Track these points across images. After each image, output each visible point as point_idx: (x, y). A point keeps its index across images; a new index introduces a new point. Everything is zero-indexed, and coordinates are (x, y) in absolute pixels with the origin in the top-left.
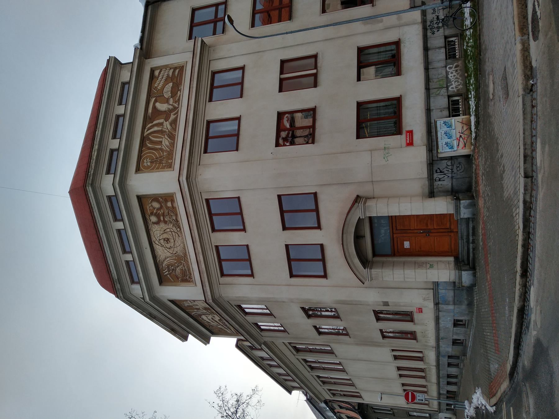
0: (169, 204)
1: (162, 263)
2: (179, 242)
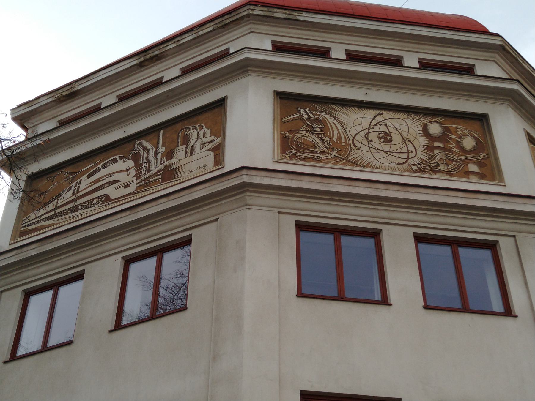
0: (473, 168)
1: (329, 114)
2: (383, 159)
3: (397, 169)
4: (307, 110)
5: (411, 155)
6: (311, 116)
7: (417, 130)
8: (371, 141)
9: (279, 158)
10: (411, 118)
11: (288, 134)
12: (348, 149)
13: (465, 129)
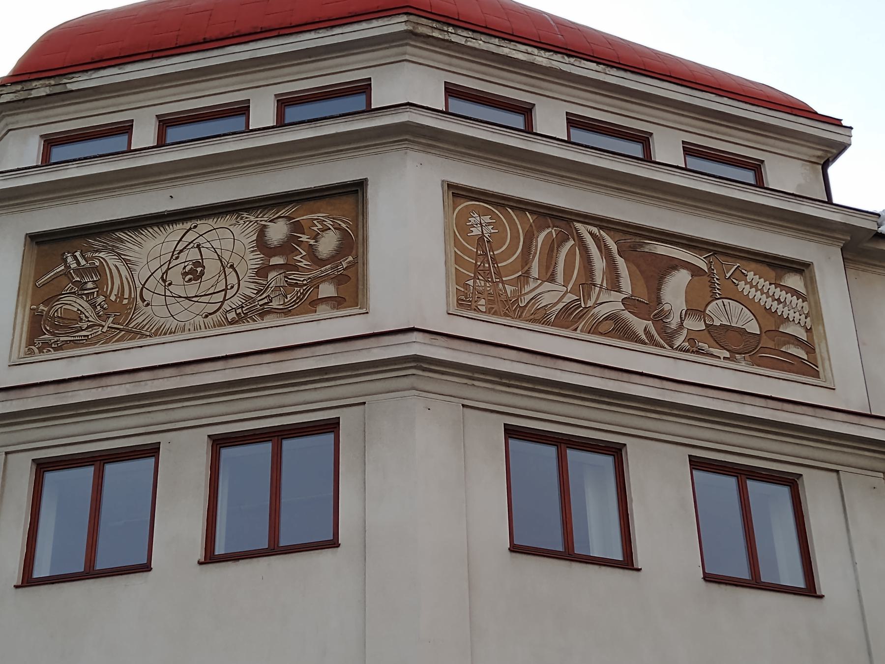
0: (327, 290)
1: (112, 250)
2: (186, 313)
3: (203, 326)
4: (78, 254)
5: (230, 293)
6: (83, 262)
7: (246, 241)
8: (170, 284)
9: (22, 355)
10: (242, 222)
11: (42, 307)
12: (131, 309)
13: (327, 217)
